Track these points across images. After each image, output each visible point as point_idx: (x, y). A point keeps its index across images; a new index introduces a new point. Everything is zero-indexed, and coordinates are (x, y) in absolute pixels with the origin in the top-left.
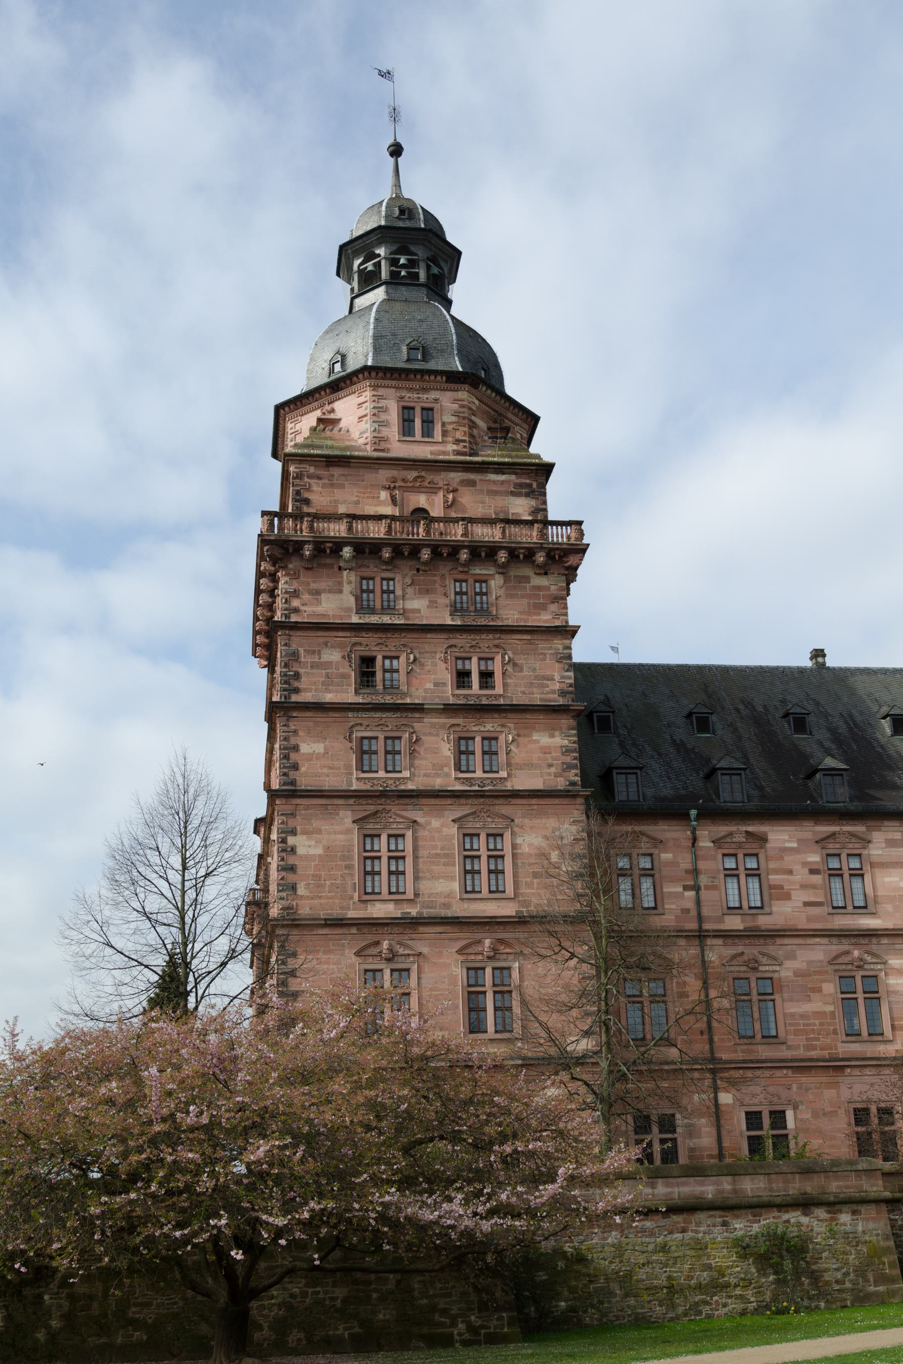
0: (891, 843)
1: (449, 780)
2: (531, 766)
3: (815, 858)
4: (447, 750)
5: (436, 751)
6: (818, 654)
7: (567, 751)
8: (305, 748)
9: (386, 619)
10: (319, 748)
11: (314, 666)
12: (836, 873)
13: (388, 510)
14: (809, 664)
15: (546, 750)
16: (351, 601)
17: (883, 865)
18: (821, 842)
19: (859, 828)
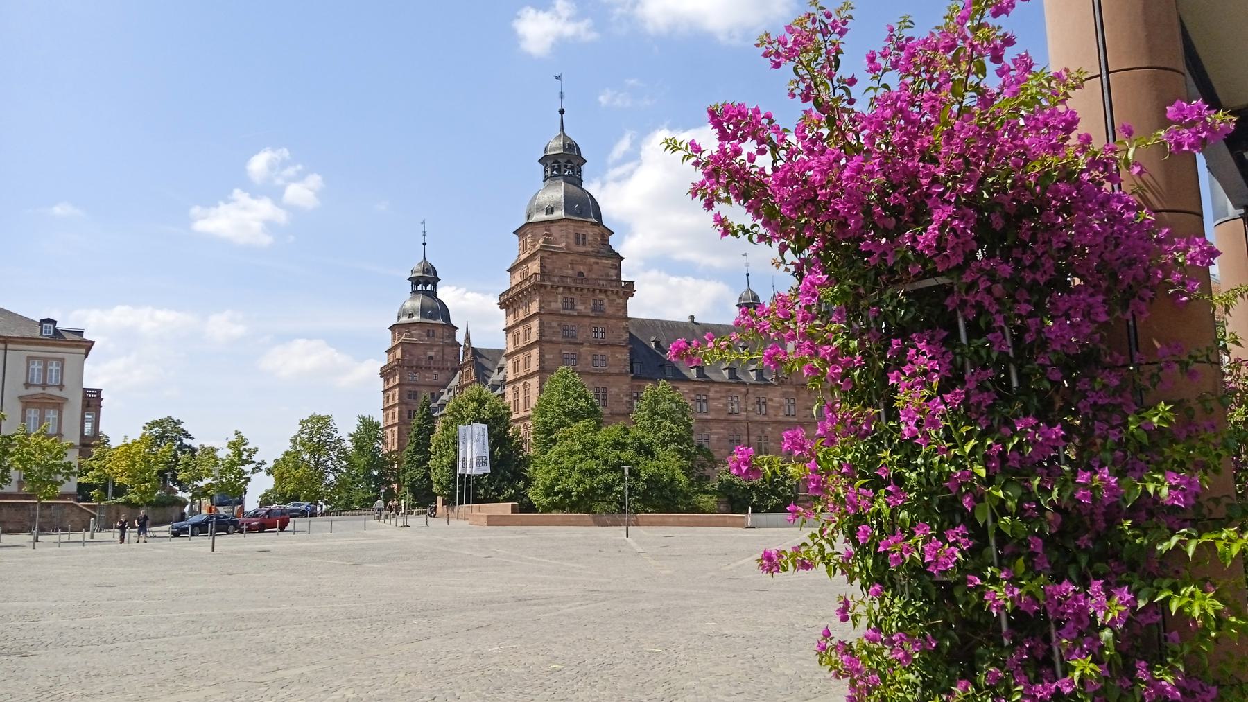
0: (716, 392)
1: (592, 369)
2: (615, 365)
3: (693, 396)
4: (590, 359)
5: (587, 359)
6: (692, 317)
7: (625, 360)
8: (547, 356)
9: (572, 312)
10: (551, 356)
11: (550, 328)
12: (699, 401)
13: (570, 272)
14: (688, 321)
15: (619, 360)
17: (713, 399)
18: (695, 390)
19: (707, 386)
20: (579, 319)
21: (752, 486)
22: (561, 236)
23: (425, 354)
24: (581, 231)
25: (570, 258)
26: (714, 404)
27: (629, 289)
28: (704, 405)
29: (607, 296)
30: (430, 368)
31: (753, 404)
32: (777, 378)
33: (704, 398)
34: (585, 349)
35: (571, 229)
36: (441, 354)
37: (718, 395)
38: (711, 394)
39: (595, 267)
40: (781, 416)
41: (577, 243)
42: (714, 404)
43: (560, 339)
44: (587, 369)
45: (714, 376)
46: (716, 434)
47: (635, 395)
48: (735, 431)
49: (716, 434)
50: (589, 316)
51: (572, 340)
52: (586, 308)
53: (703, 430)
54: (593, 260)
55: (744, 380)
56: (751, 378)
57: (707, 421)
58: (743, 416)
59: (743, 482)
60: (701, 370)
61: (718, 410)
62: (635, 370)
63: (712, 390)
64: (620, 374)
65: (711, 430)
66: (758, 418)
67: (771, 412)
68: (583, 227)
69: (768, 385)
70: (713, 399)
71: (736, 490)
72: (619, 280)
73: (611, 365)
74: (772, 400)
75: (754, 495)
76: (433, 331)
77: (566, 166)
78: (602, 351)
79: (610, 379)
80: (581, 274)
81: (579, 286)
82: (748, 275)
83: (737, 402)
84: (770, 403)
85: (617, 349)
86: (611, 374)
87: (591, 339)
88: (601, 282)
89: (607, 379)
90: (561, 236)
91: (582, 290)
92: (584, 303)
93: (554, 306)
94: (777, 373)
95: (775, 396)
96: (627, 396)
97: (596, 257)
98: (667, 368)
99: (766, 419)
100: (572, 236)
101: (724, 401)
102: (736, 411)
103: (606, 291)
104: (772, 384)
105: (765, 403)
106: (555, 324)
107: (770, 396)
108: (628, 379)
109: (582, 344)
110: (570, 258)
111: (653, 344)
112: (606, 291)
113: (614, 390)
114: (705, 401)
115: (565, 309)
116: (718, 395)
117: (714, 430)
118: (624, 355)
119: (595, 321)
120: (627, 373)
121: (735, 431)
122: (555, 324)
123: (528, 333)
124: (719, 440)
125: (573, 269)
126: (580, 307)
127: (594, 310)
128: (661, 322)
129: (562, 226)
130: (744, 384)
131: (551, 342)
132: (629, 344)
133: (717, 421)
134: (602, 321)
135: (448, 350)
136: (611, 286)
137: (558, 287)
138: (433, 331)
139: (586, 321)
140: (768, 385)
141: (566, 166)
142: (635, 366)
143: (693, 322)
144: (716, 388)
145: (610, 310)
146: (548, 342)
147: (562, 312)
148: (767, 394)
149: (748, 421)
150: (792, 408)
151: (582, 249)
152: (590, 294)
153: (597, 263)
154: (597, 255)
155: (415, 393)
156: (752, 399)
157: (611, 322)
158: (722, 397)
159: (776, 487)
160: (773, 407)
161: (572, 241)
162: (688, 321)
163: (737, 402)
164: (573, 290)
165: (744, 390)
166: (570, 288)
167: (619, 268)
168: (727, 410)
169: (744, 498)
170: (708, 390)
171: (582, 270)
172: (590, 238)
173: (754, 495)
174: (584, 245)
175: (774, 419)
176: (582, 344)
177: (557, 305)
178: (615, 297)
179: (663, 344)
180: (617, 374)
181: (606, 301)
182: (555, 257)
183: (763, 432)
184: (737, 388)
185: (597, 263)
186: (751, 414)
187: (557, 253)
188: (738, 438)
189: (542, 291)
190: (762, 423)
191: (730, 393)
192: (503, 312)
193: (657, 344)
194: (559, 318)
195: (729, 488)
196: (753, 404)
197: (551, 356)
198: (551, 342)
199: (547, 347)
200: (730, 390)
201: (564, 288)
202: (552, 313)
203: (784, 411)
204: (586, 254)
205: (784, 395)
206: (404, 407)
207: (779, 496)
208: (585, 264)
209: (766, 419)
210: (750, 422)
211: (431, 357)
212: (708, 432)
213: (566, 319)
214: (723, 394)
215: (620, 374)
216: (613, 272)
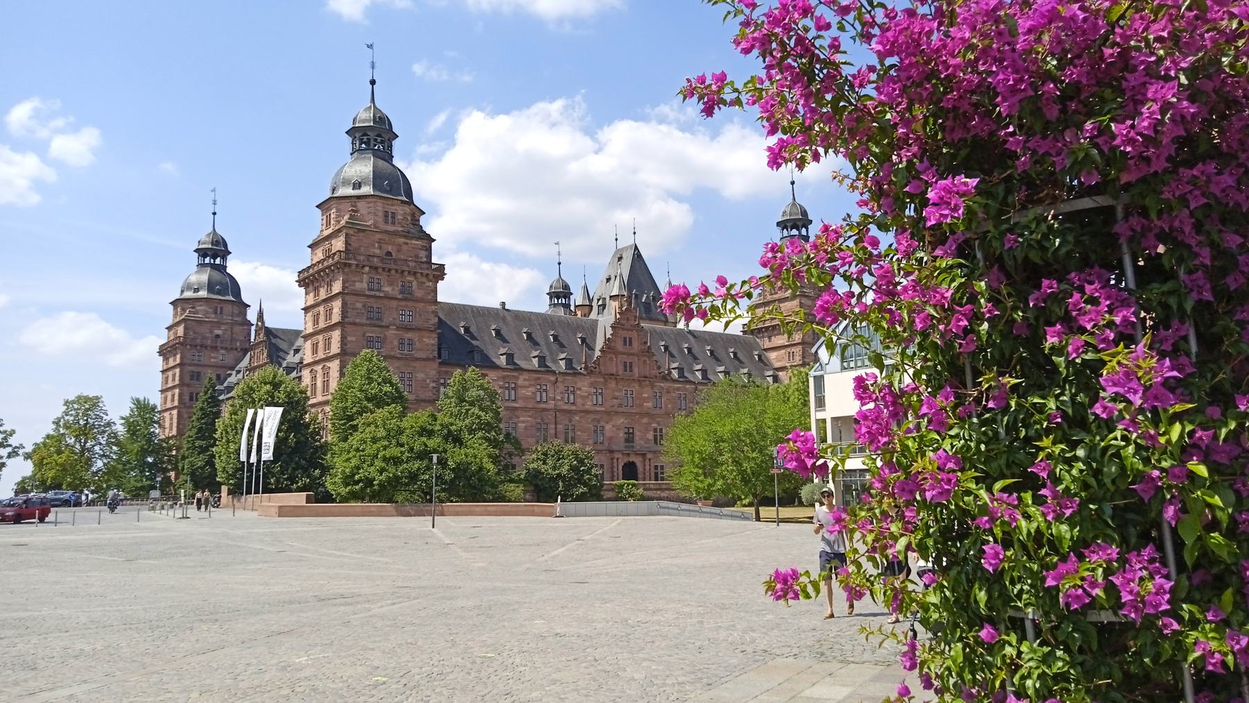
0: (525, 380)
1: (397, 353)
3: (501, 383)
4: (396, 343)
5: (392, 343)
6: (503, 304)
8: (349, 338)
9: (378, 294)
10: (354, 339)
12: (507, 388)
13: (378, 251)
14: (499, 307)
15: (427, 345)
16: (365, 285)
17: (521, 387)
19: (515, 374)
20: (385, 302)
21: (559, 475)
22: (369, 213)
23: (211, 332)
24: (392, 209)
25: (378, 236)
26: (523, 392)
27: (440, 272)
28: (513, 392)
29: (416, 278)
30: (216, 347)
31: (561, 393)
32: (586, 368)
33: (513, 386)
34: (391, 332)
35: (380, 206)
36: (229, 333)
37: (527, 383)
38: (520, 382)
39: (405, 247)
40: (589, 405)
41: (386, 222)
42: (523, 392)
43: (364, 321)
44: (392, 353)
45: (523, 364)
46: (523, 422)
47: (442, 381)
48: (542, 419)
49: (523, 422)
50: (397, 299)
51: (377, 323)
52: (393, 290)
53: (510, 418)
54: (402, 240)
55: (554, 368)
56: (560, 367)
57: (516, 409)
58: (551, 404)
59: (550, 471)
60: (510, 357)
61: (526, 398)
62: (443, 355)
63: (521, 377)
64: (427, 359)
65: (518, 417)
66: (566, 407)
67: (579, 401)
68: (392, 205)
69: (577, 374)
70: (521, 387)
71: (543, 478)
72: (429, 262)
73: (419, 350)
74: (580, 389)
75: (561, 484)
76: (221, 308)
77: (376, 140)
78: (409, 335)
79: (417, 364)
80: (389, 254)
81: (385, 266)
82: (559, 264)
83: (546, 391)
84: (578, 392)
85: (426, 334)
86: (417, 359)
87: (398, 322)
88: (410, 264)
89: (414, 364)
90: (369, 213)
91: (389, 270)
92: (391, 284)
93: (358, 286)
94: (586, 363)
95: (584, 386)
96: (434, 382)
97: (406, 237)
98: (476, 354)
99: (574, 408)
100: (381, 214)
101: (532, 389)
102: (544, 399)
103: (415, 273)
104: (581, 374)
105: (573, 392)
106: (359, 305)
107: (579, 385)
108: (435, 365)
109: (387, 327)
110: (378, 236)
111: (462, 330)
112: (415, 273)
113: (420, 376)
114: (513, 388)
115: (369, 290)
116: (527, 383)
117: (521, 419)
118: (431, 340)
119: (403, 303)
120: (433, 359)
121: (542, 419)
122: (359, 305)
123: (329, 313)
124: (526, 428)
125: (380, 248)
126: (387, 289)
127: (401, 293)
128: (472, 307)
129: (369, 203)
130: (554, 372)
131: (354, 324)
132: (439, 328)
133: (525, 409)
134: (410, 304)
135: (237, 329)
136: (421, 269)
137: (363, 267)
138: (221, 308)
139: (394, 303)
140: (577, 374)
141: (376, 140)
142: (443, 352)
143: (504, 308)
144: (526, 375)
145: (419, 294)
146: (350, 324)
147: (367, 293)
148: (576, 383)
149: (557, 410)
150: (600, 397)
151: (391, 228)
152: (398, 275)
153: (407, 244)
154: (407, 235)
155: (199, 373)
156: (561, 387)
157: (420, 305)
158: (531, 385)
159: (582, 475)
160: (582, 397)
161: (380, 219)
162: (499, 307)
163: (546, 391)
164: (380, 270)
165: (553, 378)
166: (376, 268)
167: (429, 250)
168: (535, 398)
169: (551, 487)
170: (517, 378)
171: (390, 250)
172: (400, 217)
173: (561, 484)
174: (393, 223)
175: (581, 408)
176: (387, 327)
177: (362, 285)
178: (424, 280)
179: (473, 329)
180: (424, 360)
181: (415, 283)
182: (361, 234)
183: (570, 421)
184: (547, 376)
185: (407, 244)
186: (560, 403)
187: (364, 231)
188: (545, 426)
189: (346, 270)
190: (570, 412)
191: (539, 382)
192: (302, 290)
193: (467, 330)
194: (363, 299)
195: (536, 476)
196: (561, 393)
197: (354, 339)
198: (354, 324)
199: (349, 329)
200: (539, 378)
201: (370, 267)
202: (356, 294)
203: (592, 400)
204: (395, 233)
205: (592, 385)
206: (185, 388)
207: (585, 485)
208: (394, 244)
209: (574, 408)
210: (559, 411)
211: (218, 336)
212: (515, 420)
213: (372, 300)
214: (533, 383)
215: (427, 359)
216: (423, 254)
